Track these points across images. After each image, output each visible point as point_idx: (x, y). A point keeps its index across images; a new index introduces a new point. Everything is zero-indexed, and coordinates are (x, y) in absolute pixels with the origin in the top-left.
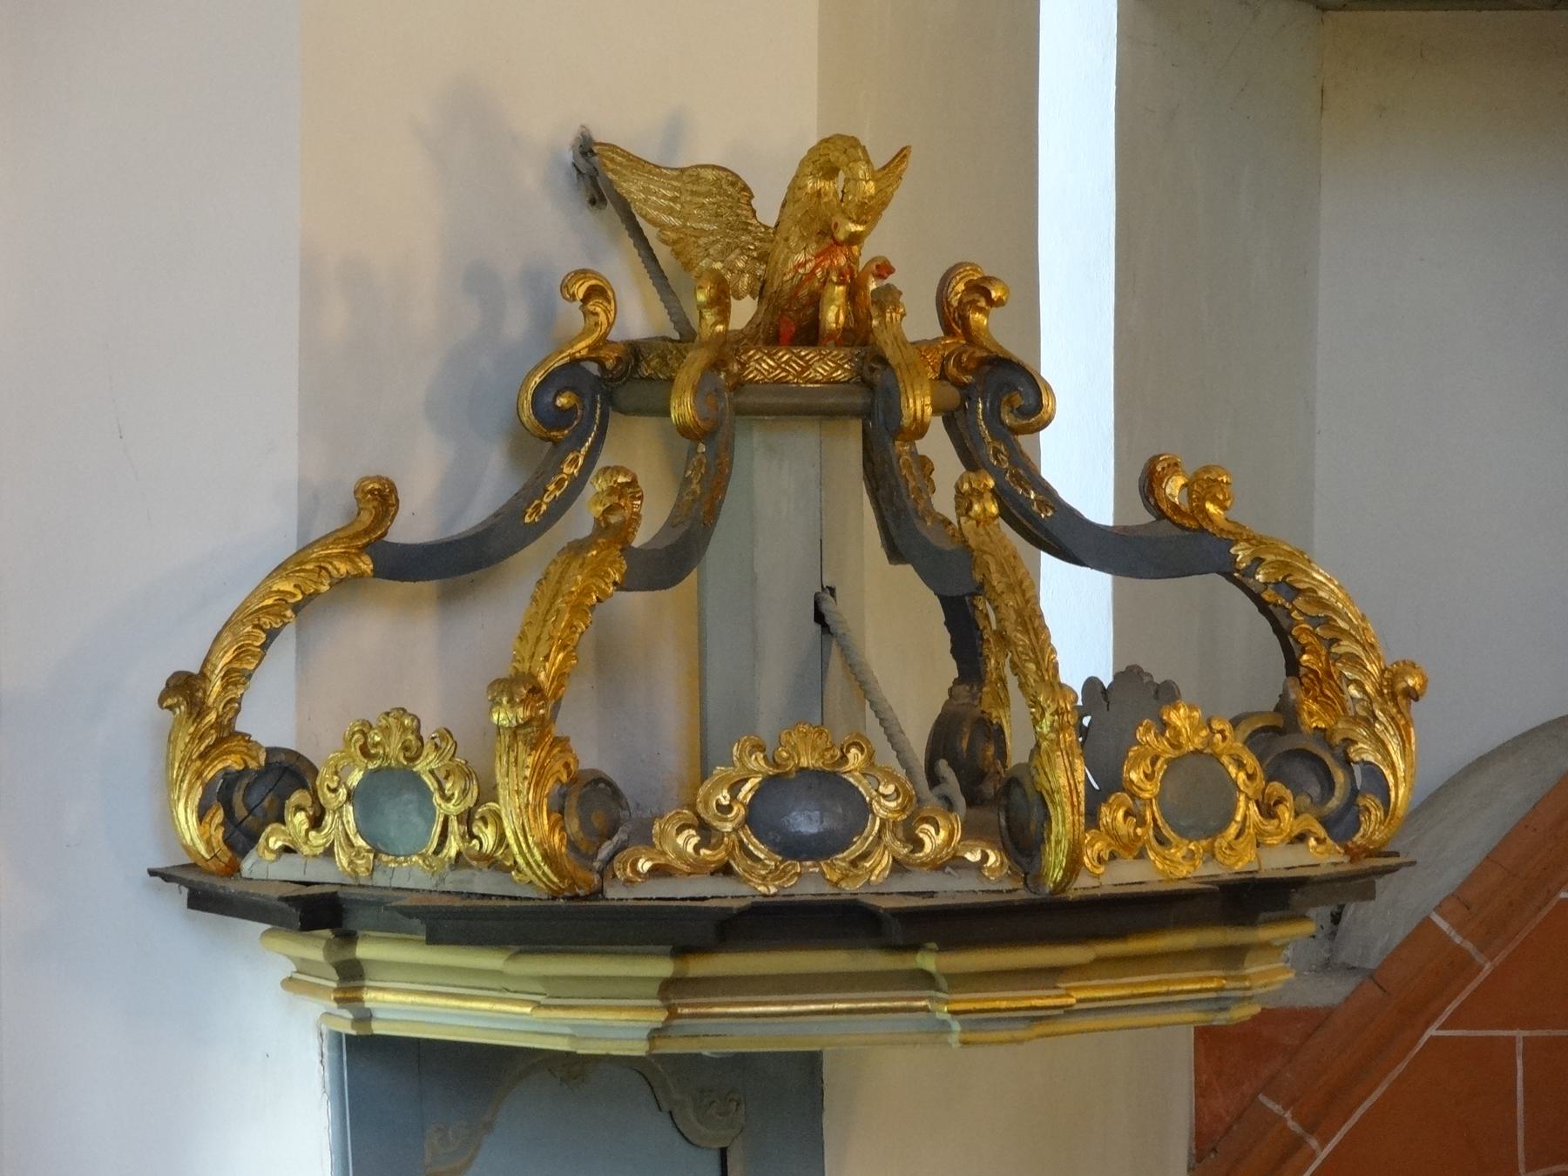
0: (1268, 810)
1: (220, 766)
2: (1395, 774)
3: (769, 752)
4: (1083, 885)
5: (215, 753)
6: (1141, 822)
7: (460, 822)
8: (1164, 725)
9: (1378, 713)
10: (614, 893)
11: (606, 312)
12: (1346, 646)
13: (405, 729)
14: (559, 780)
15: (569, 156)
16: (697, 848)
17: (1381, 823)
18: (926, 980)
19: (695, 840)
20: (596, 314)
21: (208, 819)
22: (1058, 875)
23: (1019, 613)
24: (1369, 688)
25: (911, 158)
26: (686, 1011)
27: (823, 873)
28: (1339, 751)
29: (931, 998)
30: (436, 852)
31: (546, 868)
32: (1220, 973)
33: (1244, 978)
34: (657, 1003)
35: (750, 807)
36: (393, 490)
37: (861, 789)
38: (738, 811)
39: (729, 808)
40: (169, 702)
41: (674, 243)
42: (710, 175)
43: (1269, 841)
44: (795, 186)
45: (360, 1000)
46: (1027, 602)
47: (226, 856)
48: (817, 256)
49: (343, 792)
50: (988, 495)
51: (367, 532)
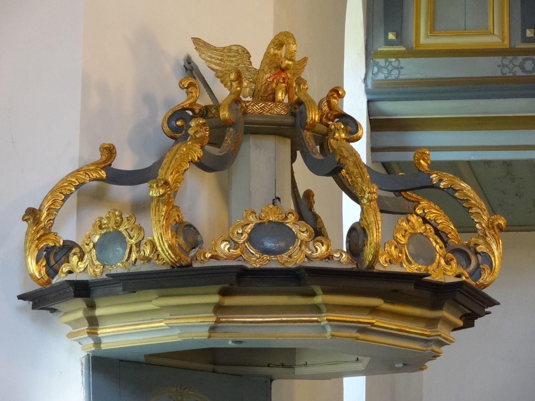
0: (448, 263)
1: (45, 244)
2: (494, 256)
3: (257, 215)
4: (378, 268)
5: (43, 238)
6: (401, 252)
7: (136, 247)
8: (408, 221)
9: (487, 234)
10: (196, 265)
11: (196, 92)
12: (474, 210)
13: (116, 216)
14: (175, 220)
15: (182, 63)
16: (229, 249)
17: (489, 274)
18: (317, 309)
19: (228, 246)
20: (192, 93)
21: (39, 263)
22: (370, 257)
23: (355, 162)
24: (483, 225)
25: (309, 61)
26: (224, 320)
27: (278, 260)
28: (472, 249)
29: (319, 317)
30: (127, 261)
31: (170, 251)
32: (429, 330)
33: (438, 331)
34: (212, 315)
35: (249, 234)
36: (114, 148)
37: (293, 229)
38: (245, 236)
39: (242, 234)
40: (26, 218)
41: (221, 77)
42: (235, 48)
43: (448, 273)
44: (267, 53)
45: (97, 334)
46: (358, 159)
47: (46, 278)
48: (274, 75)
49: (91, 245)
50: (341, 130)
51: (104, 162)
